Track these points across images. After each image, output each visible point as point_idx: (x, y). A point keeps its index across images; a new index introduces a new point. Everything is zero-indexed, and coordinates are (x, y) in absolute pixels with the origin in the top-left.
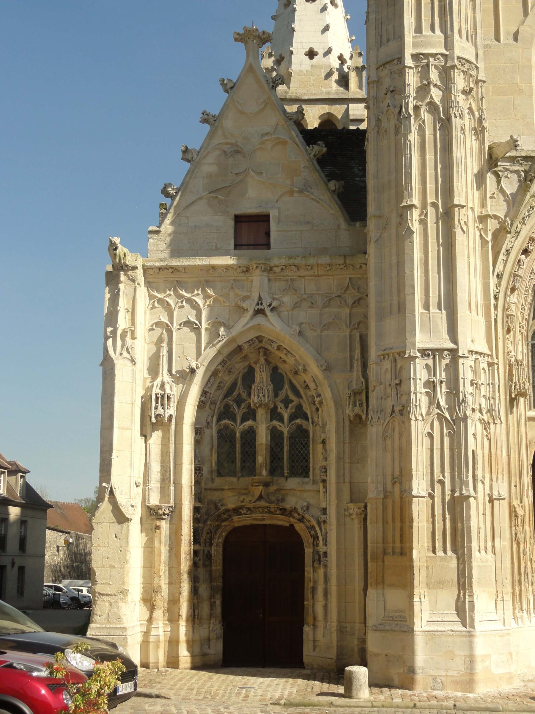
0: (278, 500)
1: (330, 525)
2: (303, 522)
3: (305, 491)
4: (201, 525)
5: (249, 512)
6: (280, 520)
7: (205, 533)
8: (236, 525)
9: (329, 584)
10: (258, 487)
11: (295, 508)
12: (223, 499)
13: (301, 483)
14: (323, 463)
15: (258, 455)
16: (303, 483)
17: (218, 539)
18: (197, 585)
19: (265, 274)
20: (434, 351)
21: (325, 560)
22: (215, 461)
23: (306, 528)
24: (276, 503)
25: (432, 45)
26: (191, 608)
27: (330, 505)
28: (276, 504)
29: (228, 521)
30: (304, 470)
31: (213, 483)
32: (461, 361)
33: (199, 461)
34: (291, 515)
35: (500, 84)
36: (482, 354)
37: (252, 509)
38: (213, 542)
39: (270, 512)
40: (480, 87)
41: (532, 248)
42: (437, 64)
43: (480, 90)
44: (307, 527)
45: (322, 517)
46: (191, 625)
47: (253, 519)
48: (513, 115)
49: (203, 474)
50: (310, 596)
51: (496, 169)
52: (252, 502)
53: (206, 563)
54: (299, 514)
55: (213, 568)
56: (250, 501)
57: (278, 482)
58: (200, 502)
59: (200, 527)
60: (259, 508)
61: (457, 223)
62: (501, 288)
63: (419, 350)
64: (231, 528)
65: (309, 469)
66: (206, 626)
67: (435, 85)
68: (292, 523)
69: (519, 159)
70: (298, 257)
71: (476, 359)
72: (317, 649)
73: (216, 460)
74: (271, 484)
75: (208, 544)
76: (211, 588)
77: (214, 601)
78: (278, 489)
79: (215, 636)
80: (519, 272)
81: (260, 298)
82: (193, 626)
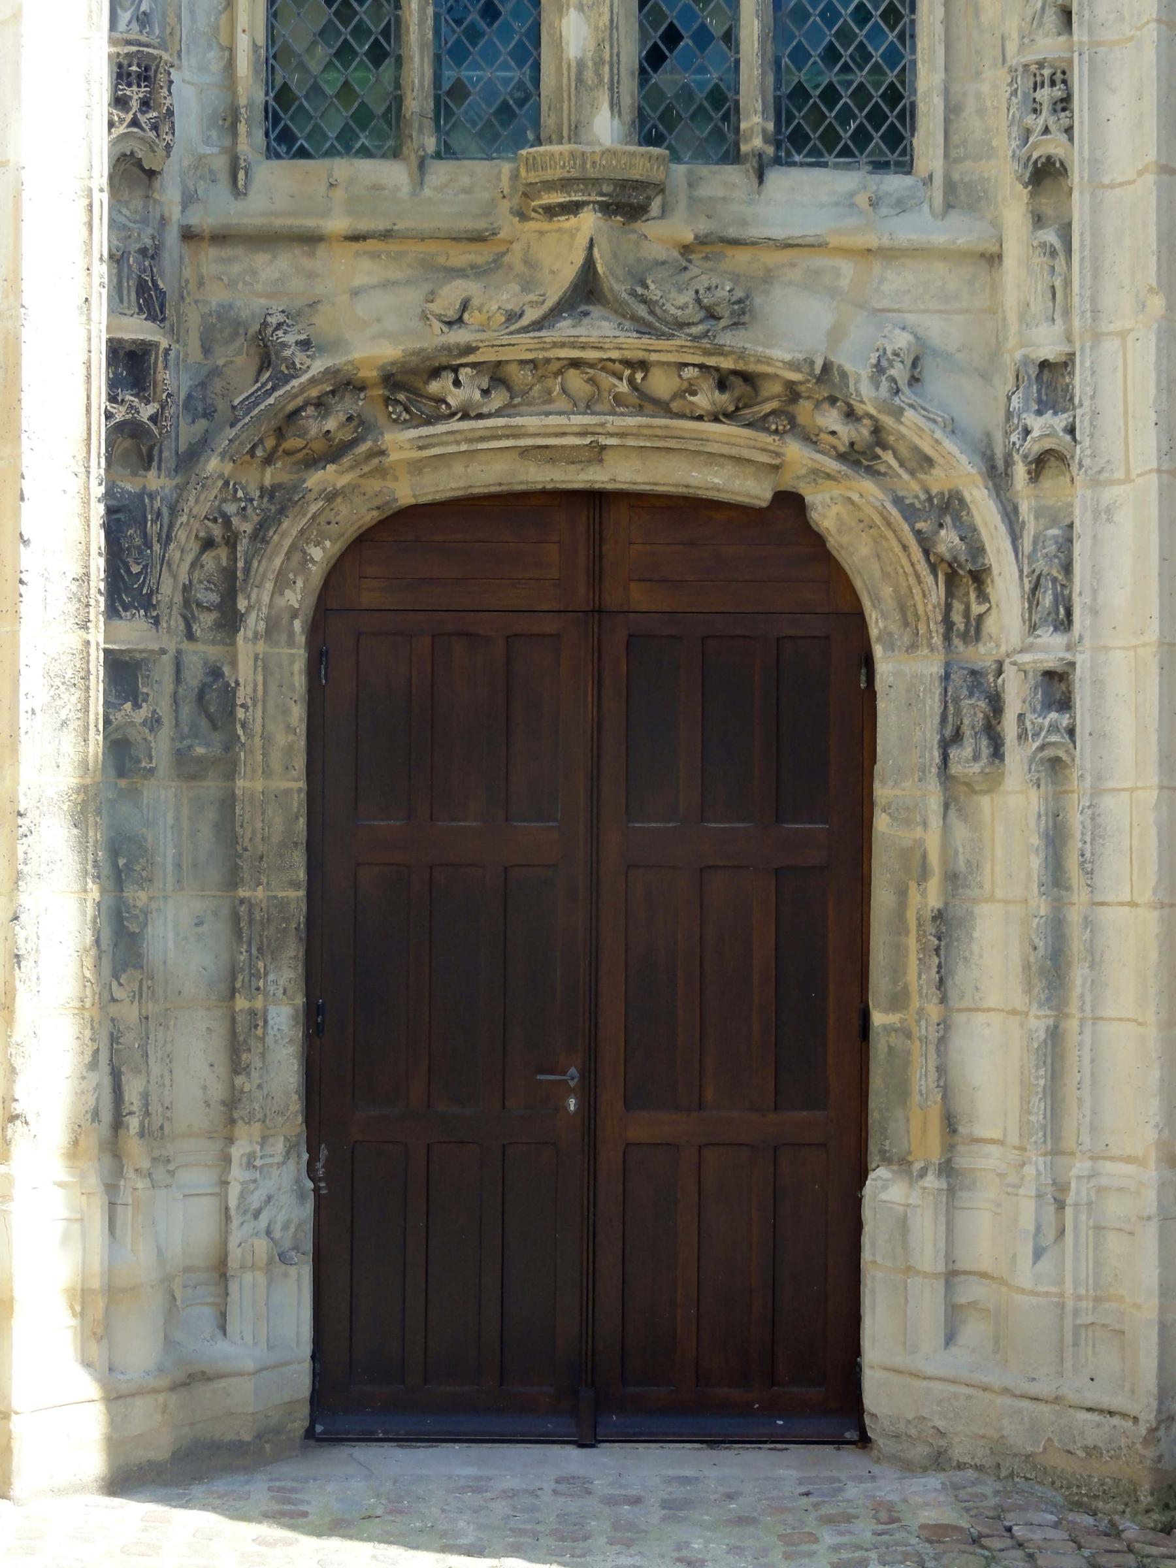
0: (711, 315)
1: (1096, 483)
2: (872, 472)
3: (888, 254)
4: (156, 481)
5: (498, 399)
6: (712, 458)
7: (185, 538)
8: (406, 493)
9: (1079, 897)
10: (568, 222)
11: (827, 367)
12: (313, 305)
13: (862, 200)
14: (1049, 46)
15: (560, 11)
16: (874, 203)
17: (282, 583)
18: (138, 896)
21: (1054, 728)
22: (255, 47)
23: (894, 512)
24: (695, 330)
26: (93, 1065)
27: (1097, 338)
28: (695, 338)
29: (347, 460)
30: (877, 116)
31: (238, 192)
33: (143, 20)
34: (792, 420)
37: (520, 377)
38: (242, 605)
39: (647, 402)
44: (898, 501)
45: (1037, 424)
46: (94, 1182)
47: (525, 452)
49: (170, 113)
50: (916, 976)
52: (525, 321)
53: (200, 750)
54: (850, 415)
55: (240, 783)
56: (513, 316)
57: (704, 191)
58: (152, 317)
59: (152, 497)
60: (572, 373)
64: (370, 517)
65: (909, 116)
66: (199, 1177)
68: (787, 482)
72: (973, 1331)
73: (261, 39)
74: (655, 206)
75: (207, 619)
76: (236, 918)
77: (252, 1013)
78: (702, 241)
79: (262, 1246)
82: (111, 1189)
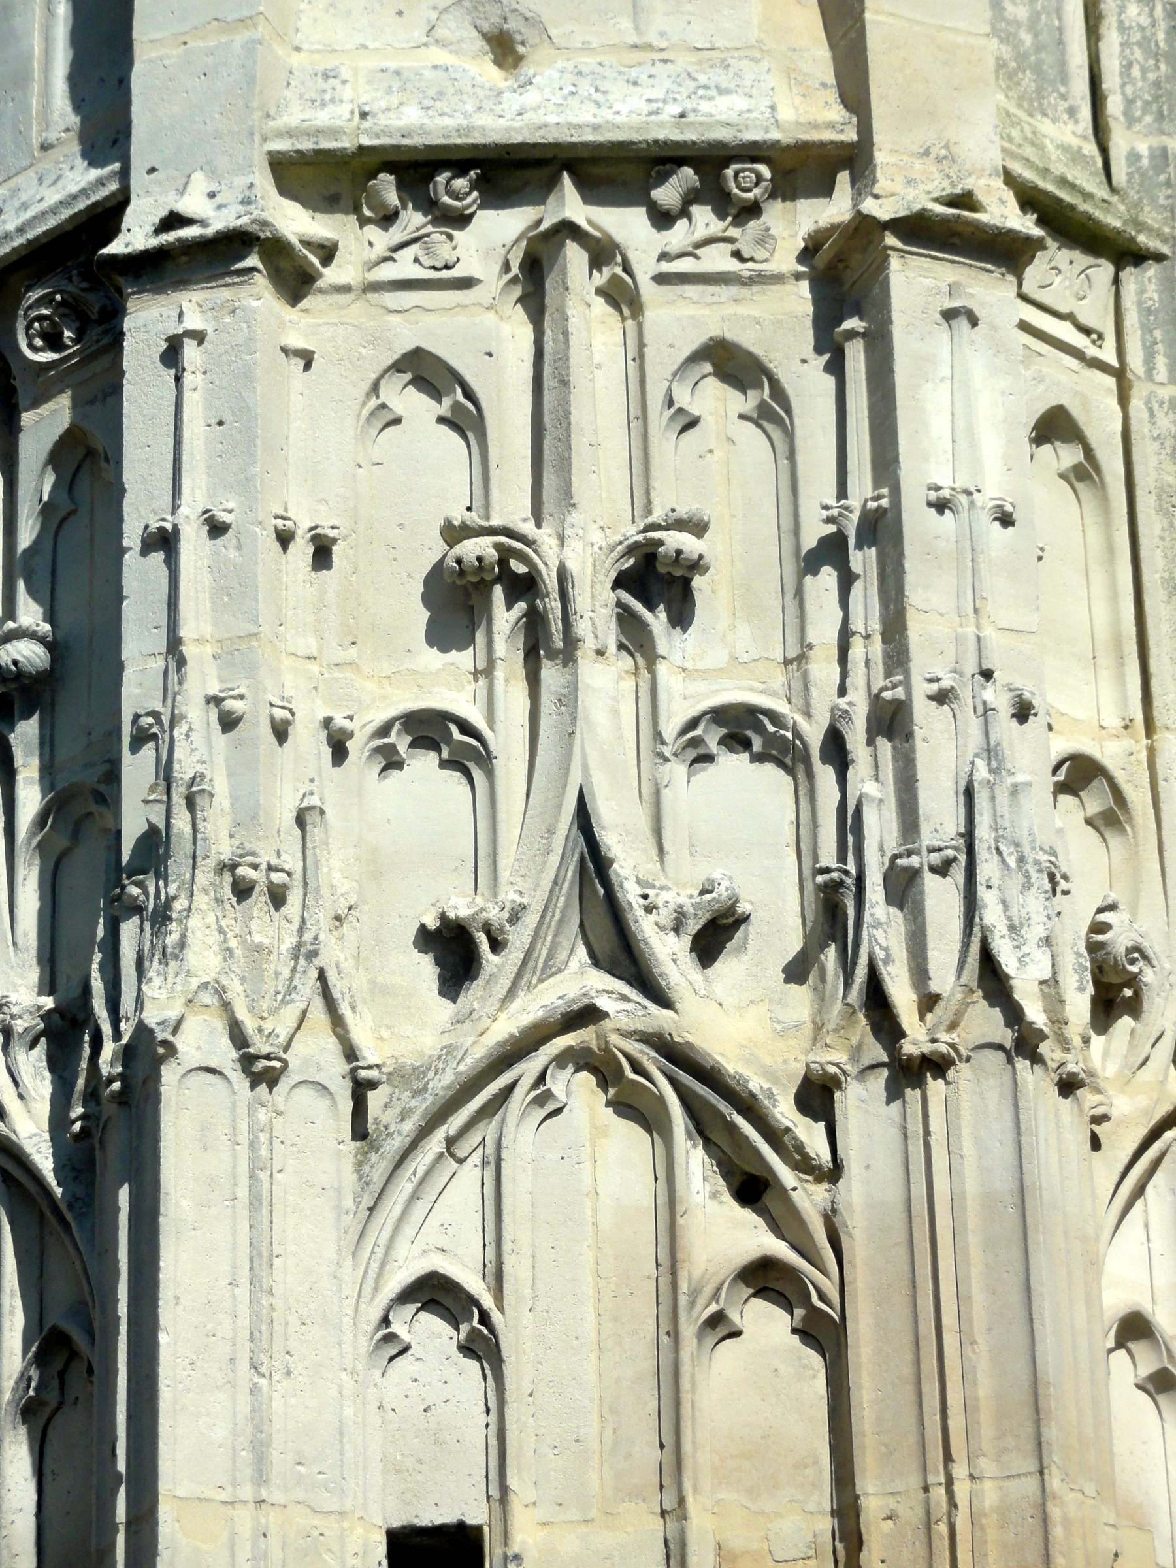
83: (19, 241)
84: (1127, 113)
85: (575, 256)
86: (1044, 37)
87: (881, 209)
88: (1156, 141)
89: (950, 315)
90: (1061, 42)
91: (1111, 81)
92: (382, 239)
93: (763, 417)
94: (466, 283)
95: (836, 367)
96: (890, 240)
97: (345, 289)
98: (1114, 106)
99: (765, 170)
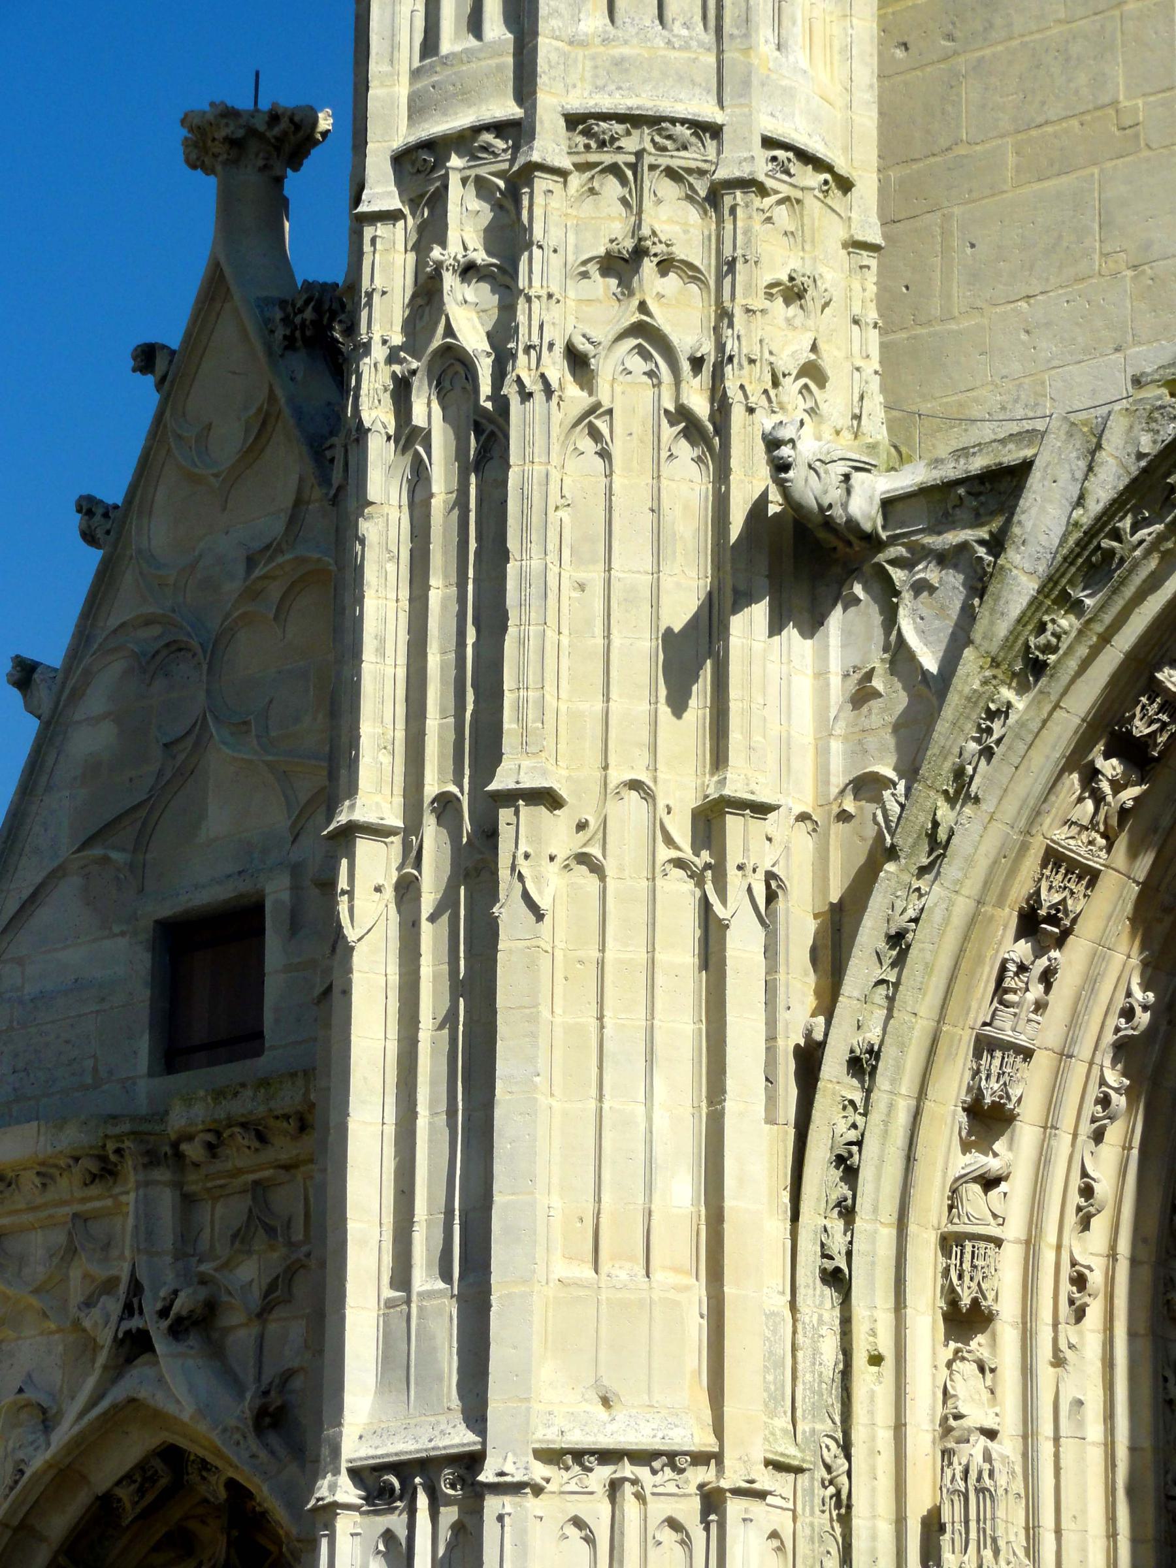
19: (162, 1174)
20: (403, 1468)
25: (465, 95)
32: (492, 1505)
35: (1047, 123)
36: (656, 1454)
40: (726, 212)
41: (1056, 898)
42: (483, 172)
43: (729, 226)
48: (1096, 257)
51: (881, 558)
61: (504, 873)
62: (876, 1116)
63: (356, 1474)
67: (468, 271)
69: (961, 491)
70: (243, 1085)
71: (614, 1487)
80: (997, 1023)
81: (136, 1287)
83: (443, 1452)
84: (803, 1416)
85: (628, 1488)
86: (778, 1385)
87: (725, 1484)
88: (811, 1425)
89: (744, 1520)
90: (783, 1386)
91: (798, 1404)
92: (566, 1475)
93: (682, 1542)
94: (592, 1493)
95: (707, 1529)
96: (728, 1494)
97: (553, 1493)
98: (799, 1413)
99: (688, 1458)
